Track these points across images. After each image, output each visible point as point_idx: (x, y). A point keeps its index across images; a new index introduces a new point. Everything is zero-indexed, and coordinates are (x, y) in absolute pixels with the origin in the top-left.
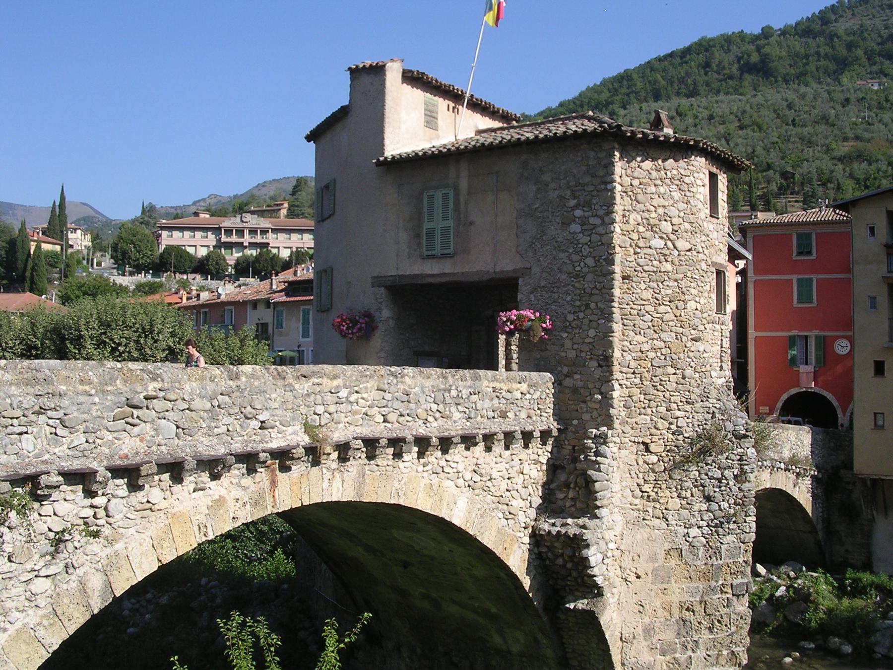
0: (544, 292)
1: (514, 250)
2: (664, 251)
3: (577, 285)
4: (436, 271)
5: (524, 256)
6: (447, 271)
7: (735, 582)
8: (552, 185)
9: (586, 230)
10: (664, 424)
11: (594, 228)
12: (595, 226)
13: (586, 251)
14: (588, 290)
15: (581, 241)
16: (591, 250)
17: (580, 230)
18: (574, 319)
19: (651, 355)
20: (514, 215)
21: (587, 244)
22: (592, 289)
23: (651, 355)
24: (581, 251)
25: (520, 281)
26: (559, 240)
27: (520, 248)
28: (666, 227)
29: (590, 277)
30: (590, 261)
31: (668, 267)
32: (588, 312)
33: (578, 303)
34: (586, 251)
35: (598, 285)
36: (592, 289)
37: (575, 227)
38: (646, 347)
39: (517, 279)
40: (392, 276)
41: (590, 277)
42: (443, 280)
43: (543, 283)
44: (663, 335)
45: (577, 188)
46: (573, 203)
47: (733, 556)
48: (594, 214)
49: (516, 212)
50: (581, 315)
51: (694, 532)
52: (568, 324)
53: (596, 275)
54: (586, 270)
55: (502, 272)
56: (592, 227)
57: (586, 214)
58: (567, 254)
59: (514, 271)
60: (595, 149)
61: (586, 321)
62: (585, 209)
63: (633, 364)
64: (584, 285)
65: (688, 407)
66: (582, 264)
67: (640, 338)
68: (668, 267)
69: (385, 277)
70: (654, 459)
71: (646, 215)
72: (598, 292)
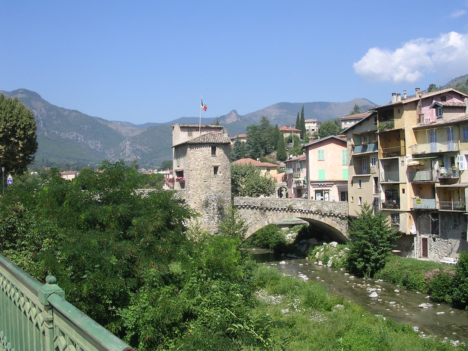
2: (198, 165)
7: (214, 230)
10: (198, 198)
19: (196, 185)
23: (196, 185)
28: (199, 160)
31: (199, 168)
38: (195, 184)
42: (178, 171)
44: (198, 181)
47: (213, 225)
51: (205, 220)
63: (193, 187)
65: (203, 195)
67: (194, 182)
68: (199, 168)
70: (197, 205)
71: (195, 158)
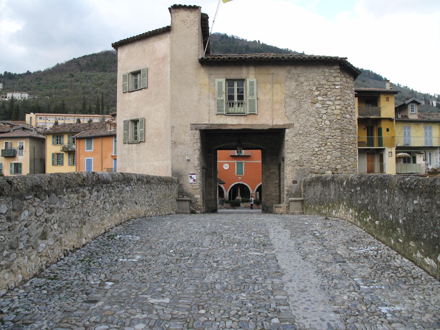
1: (283, 115)
4: (235, 123)
5: (290, 118)
6: (242, 123)
8: (305, 83)
11: (329, 106)
13: (324, 117)
16: (328, 117)
17: (321, 107)
20: (284, 97)
21: (325, 114)
22: (329, 136)
25: (287, 131)
27: (287, 114)
32: (326, 147)
33: (320, 142)
36: (329, 136)
37: (318, 105)
39: (285, 129)
40: (204, 124)
41: (327, 130)
43: (301, 132)
45: (320, 86)
46: (317, 93)
50: (323, 148)
54: (325, 126)
55: (277, 125)
56: (328, 106)
58: (315, 118)
59: (284, 125)
60: (329, 68)
61: (325, 151)
66: (323, 124)
72: (332, 137)
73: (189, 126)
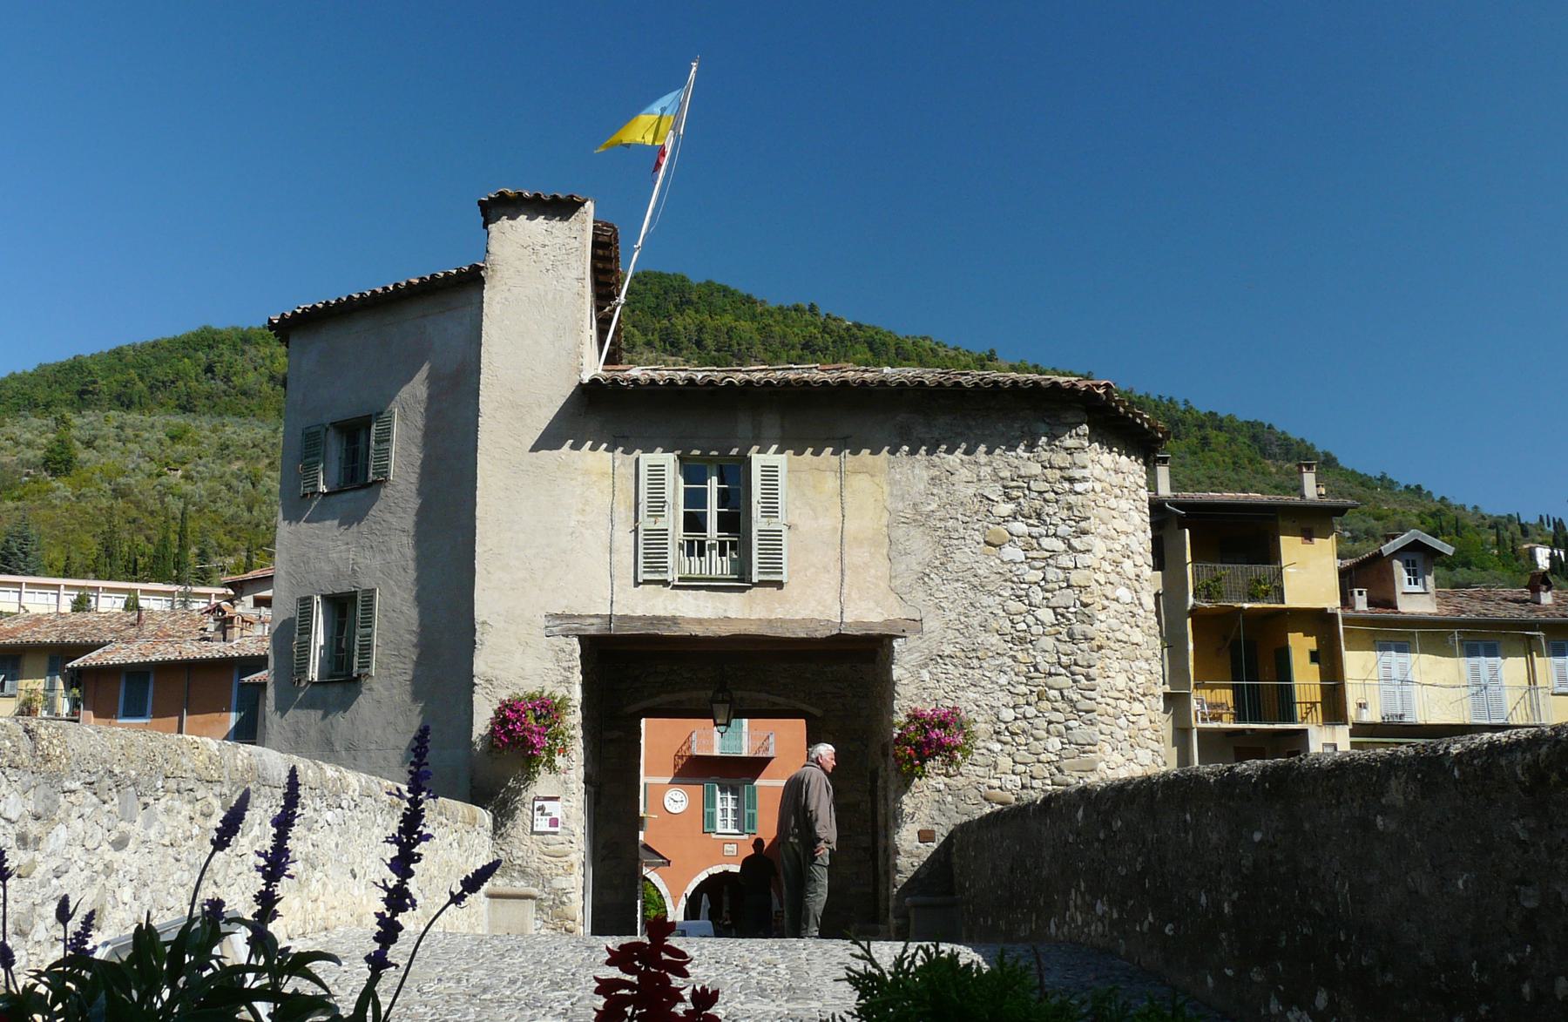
0: (950, 667)
1: (883, 585)
3: (1020, 656)
4: (707, 613)
9: (1033, 559)
12: (1054, 553)
13: (1037, 596)
14: (1043, 667)
15: (1027, 578)
16: (1049, 595)
18: (1016, 719)
20: (884, 521)
21: (1036, 583)
22: (1052, 664)
24: (1027, 595)
26: (980, 572)
29: (1048, 642)
30: (1047, 615)
33: (1023, 689)
34: (1037, 596)
35: (1064, 659)
37: (1013, 552)
45: (1014, 484)
46: (1007, 508)
48: (1051, 532)
49: (887, 515)
50: (1031, 711)
52: (1003, 726)
53: (1058, 640)
55: (858, 624)
56: (1048, 554)
57: (1035, 531)
59: (887, 623)
62: (1031, 521)
64: (1035, 657)
69: (580, 616)
73: (543, 622)
